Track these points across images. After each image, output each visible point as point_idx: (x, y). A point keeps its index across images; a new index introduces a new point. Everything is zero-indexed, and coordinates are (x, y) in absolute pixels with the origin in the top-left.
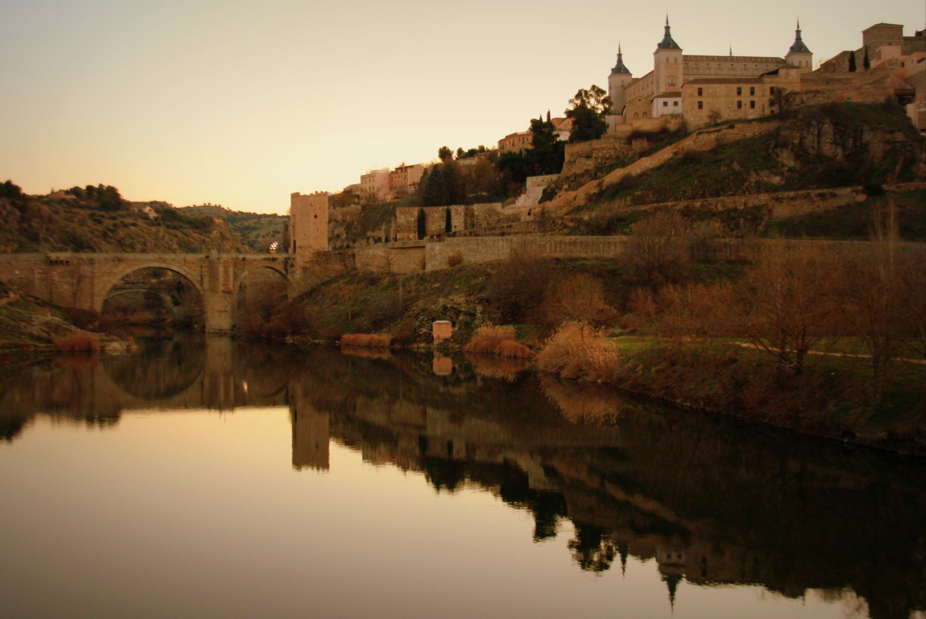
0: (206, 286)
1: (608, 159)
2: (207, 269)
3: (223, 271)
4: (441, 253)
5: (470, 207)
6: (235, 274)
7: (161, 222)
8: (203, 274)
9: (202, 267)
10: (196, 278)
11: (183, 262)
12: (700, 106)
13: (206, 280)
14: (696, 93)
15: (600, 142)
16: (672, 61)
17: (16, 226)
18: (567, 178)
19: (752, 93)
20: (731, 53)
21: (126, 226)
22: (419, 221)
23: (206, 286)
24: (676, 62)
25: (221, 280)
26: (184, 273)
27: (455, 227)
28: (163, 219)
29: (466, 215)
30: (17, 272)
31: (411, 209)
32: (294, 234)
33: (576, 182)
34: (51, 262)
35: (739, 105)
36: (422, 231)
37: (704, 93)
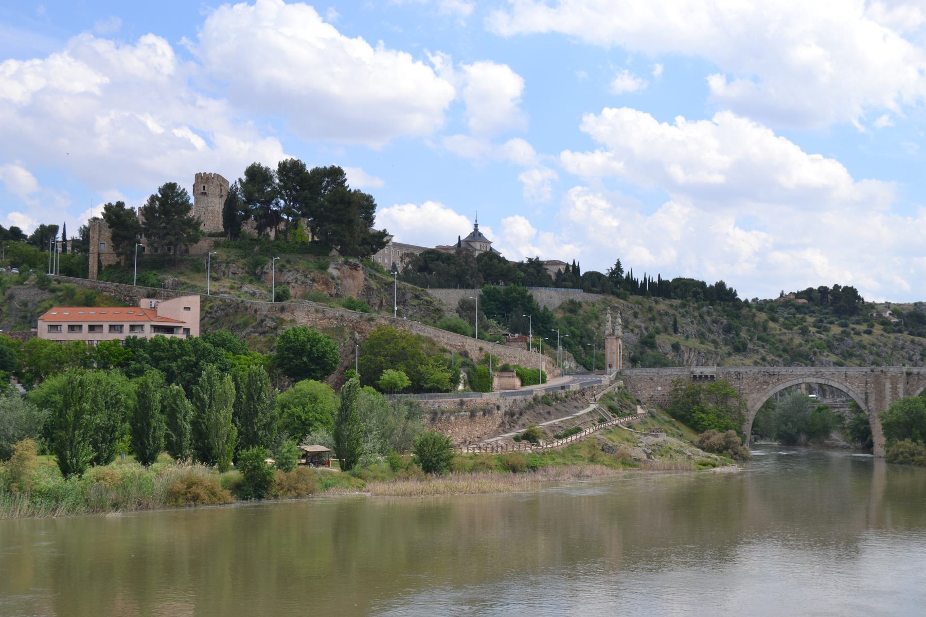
0: (872, 404)
2: (873, 385)
3: (890, 388)
7: (903, 328)
8: (868, 391)
9: (866, 384)
10: (860, 395)
11: (844, 377)
13: (872, 398)
21: (858, 333)
26: (845, 390)
28: (906, 325)
30: (660, 388)
34: (695, 377)
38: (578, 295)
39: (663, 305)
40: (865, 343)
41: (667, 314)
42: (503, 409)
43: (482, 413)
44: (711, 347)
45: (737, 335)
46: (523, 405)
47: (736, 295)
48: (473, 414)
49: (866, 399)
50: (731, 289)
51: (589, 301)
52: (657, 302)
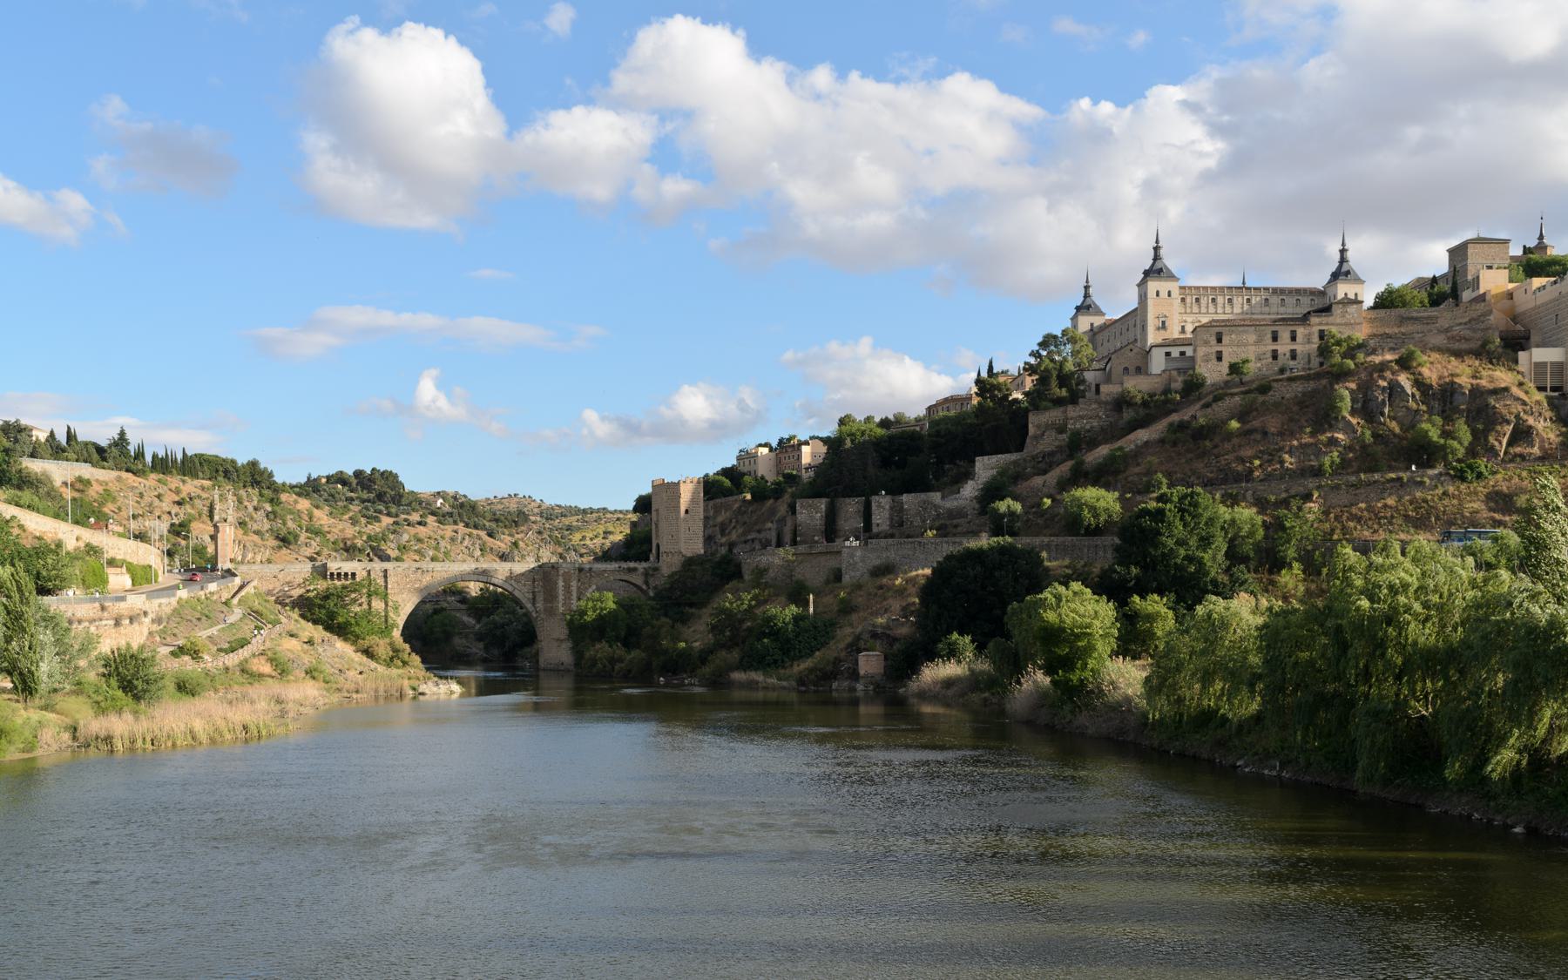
0: (540, 605)
1: (1089, 431)
4: (863, 561)
5: (898, 498)
6: (579, 588)
9: (534, 582)
12: (1219, 358)
13: (540, 598)
14: (1213, 340)
15: (1078, 409)
16: (1164, 294)
17: (267, 526)
18: (1034, 458)
19: (1293, 338)
20: (1244, 283)
22: (827, 516)
23: (540, 605)
24: (1169, 295)
25: (561, 597)
27: (878, 525)
29: (891, 508)
31: (816, 500)
32: (657, 536)
33: (1045, 463)
35: (1275, 355)
36: (831, 531)
37: (1225, 339)
38: (86, 470)
39: (191, 486)
40: (421, 536)
41: (199, 497)
42: (151, 616)
43: (127, 621)
44: (256, 538)
45: (284, 524)
46: (168, 610)
47: (273, 476)
48: (117, 623)
49: (534, 599)
50: (266, 469)
51: (101, 478)
52: (184, 481)
